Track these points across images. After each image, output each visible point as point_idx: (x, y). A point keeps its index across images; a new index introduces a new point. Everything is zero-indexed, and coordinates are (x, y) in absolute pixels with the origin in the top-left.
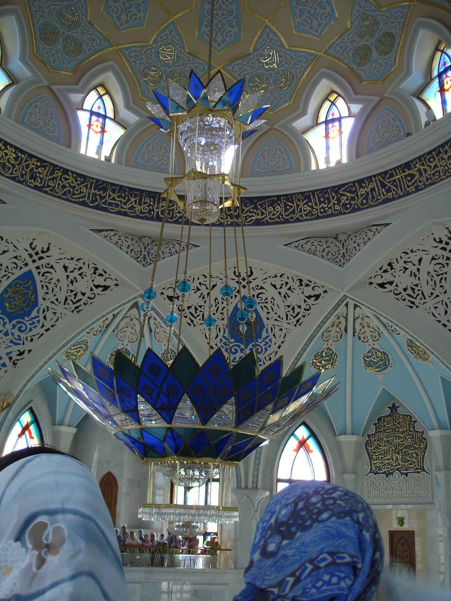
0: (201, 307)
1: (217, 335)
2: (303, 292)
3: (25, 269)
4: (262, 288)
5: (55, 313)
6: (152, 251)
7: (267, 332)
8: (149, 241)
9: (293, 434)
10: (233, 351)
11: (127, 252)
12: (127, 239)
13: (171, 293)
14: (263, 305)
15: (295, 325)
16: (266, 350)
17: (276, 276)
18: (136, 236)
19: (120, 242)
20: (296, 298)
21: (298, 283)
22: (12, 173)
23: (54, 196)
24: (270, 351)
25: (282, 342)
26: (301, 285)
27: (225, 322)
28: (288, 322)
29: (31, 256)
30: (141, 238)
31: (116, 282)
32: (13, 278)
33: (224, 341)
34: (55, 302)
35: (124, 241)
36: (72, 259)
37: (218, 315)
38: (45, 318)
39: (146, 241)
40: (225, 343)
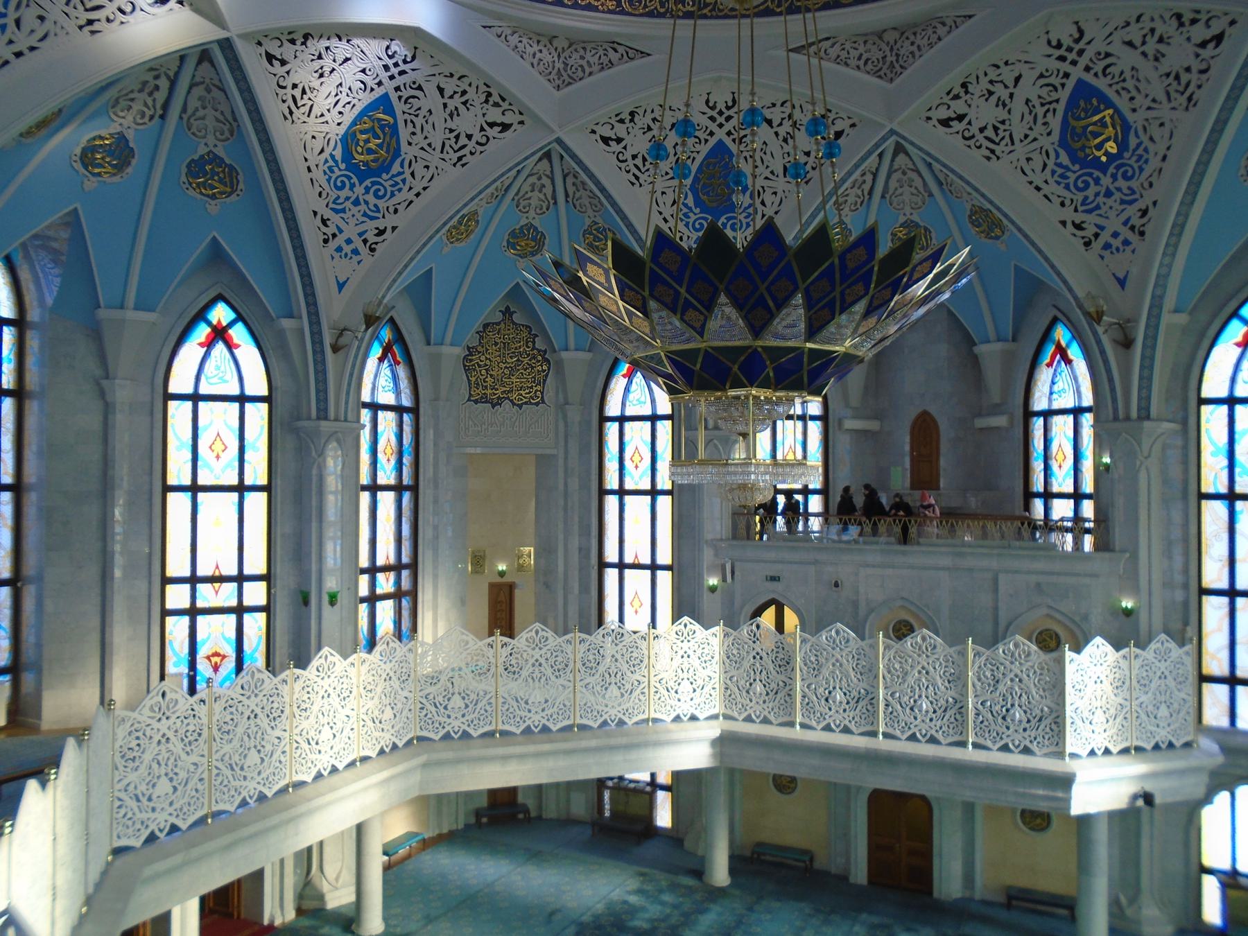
0: (1003, 122)
1: (1045, 165)
2: (1189, 39)
3: (713, 141)
4: (1108, 55)
5: (775, 193)
6: (902, 52)
7: (1137, 136)
8: (896, 35)
9: (1235, 314)
10: (1080, 185)
11: (858, 67)
12: (856, 45)
13: (943, 113)
14: (1118, 87)
15: (1187, 109)
16: (1141, 169)
17: (1128, 24)
18: (872, 33)
19: (844, 54)
20: (1179, 55)
21: (1174, 23)
22: (646, 6)
23: (717, 17)
24: (1148, 169)
25: (1168, 148)
26: (1181, 24)
27: (1056, 136)
28: (1173, 104)
29: (712, 119)
30: (880, 35)
31: (851, 122)
32: (699, 159)
33: (1060, 171)
34: (770, 176)
35: (851, 51)
36: (774, 105)
37: (1039, 128)
38: (763, 203)
39: (890, 37)
40: (1062, 176)
